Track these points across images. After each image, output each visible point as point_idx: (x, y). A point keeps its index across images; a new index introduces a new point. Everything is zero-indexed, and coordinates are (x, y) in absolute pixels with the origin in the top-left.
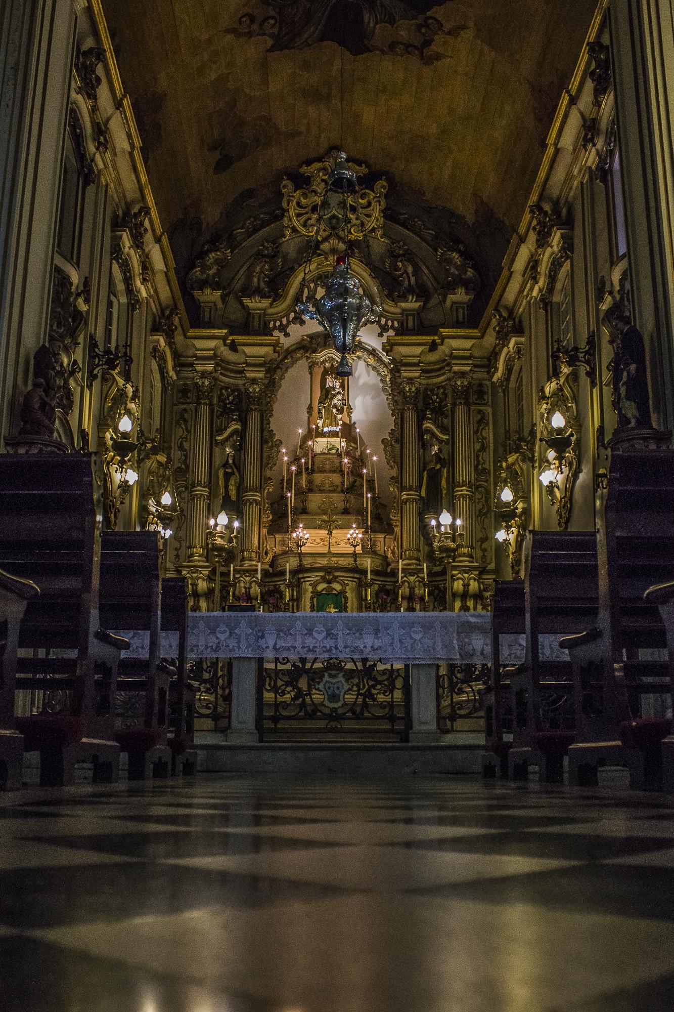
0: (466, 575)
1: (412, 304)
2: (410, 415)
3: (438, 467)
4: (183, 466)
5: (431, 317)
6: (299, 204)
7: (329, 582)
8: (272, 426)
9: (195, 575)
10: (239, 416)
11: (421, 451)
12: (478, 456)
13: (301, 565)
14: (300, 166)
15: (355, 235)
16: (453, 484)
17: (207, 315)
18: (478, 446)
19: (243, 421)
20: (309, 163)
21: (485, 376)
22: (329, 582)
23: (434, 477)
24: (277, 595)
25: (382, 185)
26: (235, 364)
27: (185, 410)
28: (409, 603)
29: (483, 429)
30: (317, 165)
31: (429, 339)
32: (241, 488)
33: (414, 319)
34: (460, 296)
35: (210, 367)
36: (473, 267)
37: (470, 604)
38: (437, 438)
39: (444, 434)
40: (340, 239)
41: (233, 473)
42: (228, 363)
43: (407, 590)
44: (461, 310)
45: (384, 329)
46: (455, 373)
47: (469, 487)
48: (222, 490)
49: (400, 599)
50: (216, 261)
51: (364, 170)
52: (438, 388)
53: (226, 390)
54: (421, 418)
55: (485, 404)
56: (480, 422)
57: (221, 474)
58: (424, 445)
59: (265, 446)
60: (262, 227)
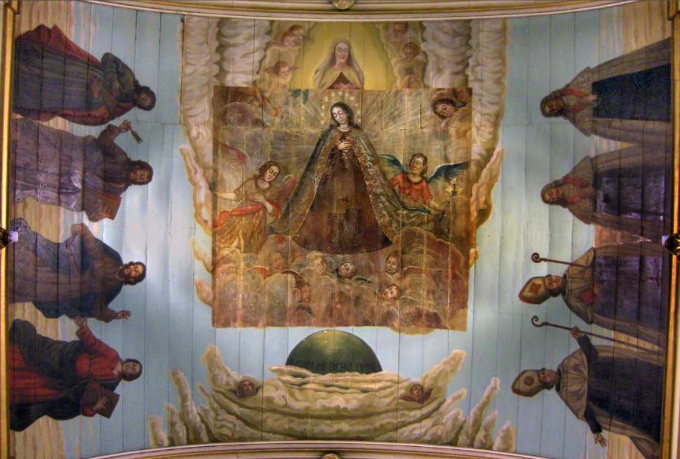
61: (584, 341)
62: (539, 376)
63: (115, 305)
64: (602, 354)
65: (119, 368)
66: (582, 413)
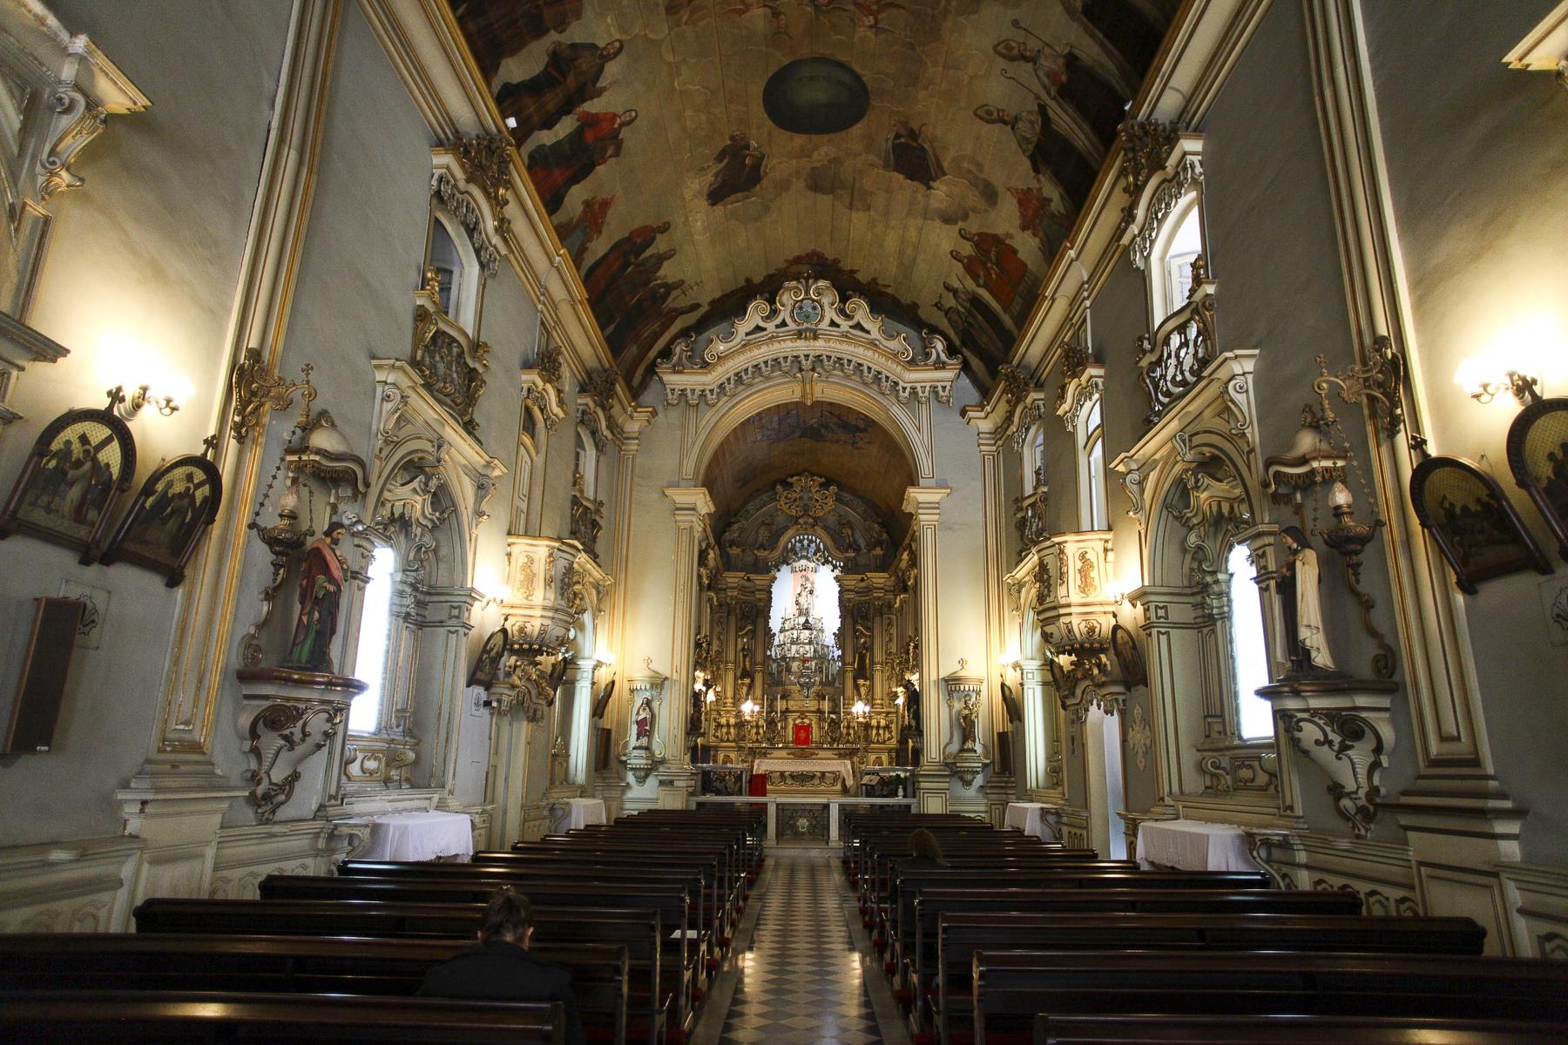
2: (849, 621)
5: (862, 560)
8: (770, 625)
13: (787, 708)
15: (820, 514)
16: (872, 663)
19: (754, 623)
20: (792, 476)
23: (862, 658)
25: (833, 488)
30: (795, 478)
32: (753, 664)
34: (878, 551)
35: (735, 594)
36: (887, 533)
37: (881, 732)
38: (864, 634)
40: (809, 516)
45: (835, 567)
51: (823, 480)
54: (855, 623)
56: (889, 624)
57: (741, 655)
58: (858, 638)
60: (764, 505)
61: (1043, 109)
62: (998, 112)
63: (600, 84)
64: (1054, 126)
65: (618, 121)
66: (1028, 154)
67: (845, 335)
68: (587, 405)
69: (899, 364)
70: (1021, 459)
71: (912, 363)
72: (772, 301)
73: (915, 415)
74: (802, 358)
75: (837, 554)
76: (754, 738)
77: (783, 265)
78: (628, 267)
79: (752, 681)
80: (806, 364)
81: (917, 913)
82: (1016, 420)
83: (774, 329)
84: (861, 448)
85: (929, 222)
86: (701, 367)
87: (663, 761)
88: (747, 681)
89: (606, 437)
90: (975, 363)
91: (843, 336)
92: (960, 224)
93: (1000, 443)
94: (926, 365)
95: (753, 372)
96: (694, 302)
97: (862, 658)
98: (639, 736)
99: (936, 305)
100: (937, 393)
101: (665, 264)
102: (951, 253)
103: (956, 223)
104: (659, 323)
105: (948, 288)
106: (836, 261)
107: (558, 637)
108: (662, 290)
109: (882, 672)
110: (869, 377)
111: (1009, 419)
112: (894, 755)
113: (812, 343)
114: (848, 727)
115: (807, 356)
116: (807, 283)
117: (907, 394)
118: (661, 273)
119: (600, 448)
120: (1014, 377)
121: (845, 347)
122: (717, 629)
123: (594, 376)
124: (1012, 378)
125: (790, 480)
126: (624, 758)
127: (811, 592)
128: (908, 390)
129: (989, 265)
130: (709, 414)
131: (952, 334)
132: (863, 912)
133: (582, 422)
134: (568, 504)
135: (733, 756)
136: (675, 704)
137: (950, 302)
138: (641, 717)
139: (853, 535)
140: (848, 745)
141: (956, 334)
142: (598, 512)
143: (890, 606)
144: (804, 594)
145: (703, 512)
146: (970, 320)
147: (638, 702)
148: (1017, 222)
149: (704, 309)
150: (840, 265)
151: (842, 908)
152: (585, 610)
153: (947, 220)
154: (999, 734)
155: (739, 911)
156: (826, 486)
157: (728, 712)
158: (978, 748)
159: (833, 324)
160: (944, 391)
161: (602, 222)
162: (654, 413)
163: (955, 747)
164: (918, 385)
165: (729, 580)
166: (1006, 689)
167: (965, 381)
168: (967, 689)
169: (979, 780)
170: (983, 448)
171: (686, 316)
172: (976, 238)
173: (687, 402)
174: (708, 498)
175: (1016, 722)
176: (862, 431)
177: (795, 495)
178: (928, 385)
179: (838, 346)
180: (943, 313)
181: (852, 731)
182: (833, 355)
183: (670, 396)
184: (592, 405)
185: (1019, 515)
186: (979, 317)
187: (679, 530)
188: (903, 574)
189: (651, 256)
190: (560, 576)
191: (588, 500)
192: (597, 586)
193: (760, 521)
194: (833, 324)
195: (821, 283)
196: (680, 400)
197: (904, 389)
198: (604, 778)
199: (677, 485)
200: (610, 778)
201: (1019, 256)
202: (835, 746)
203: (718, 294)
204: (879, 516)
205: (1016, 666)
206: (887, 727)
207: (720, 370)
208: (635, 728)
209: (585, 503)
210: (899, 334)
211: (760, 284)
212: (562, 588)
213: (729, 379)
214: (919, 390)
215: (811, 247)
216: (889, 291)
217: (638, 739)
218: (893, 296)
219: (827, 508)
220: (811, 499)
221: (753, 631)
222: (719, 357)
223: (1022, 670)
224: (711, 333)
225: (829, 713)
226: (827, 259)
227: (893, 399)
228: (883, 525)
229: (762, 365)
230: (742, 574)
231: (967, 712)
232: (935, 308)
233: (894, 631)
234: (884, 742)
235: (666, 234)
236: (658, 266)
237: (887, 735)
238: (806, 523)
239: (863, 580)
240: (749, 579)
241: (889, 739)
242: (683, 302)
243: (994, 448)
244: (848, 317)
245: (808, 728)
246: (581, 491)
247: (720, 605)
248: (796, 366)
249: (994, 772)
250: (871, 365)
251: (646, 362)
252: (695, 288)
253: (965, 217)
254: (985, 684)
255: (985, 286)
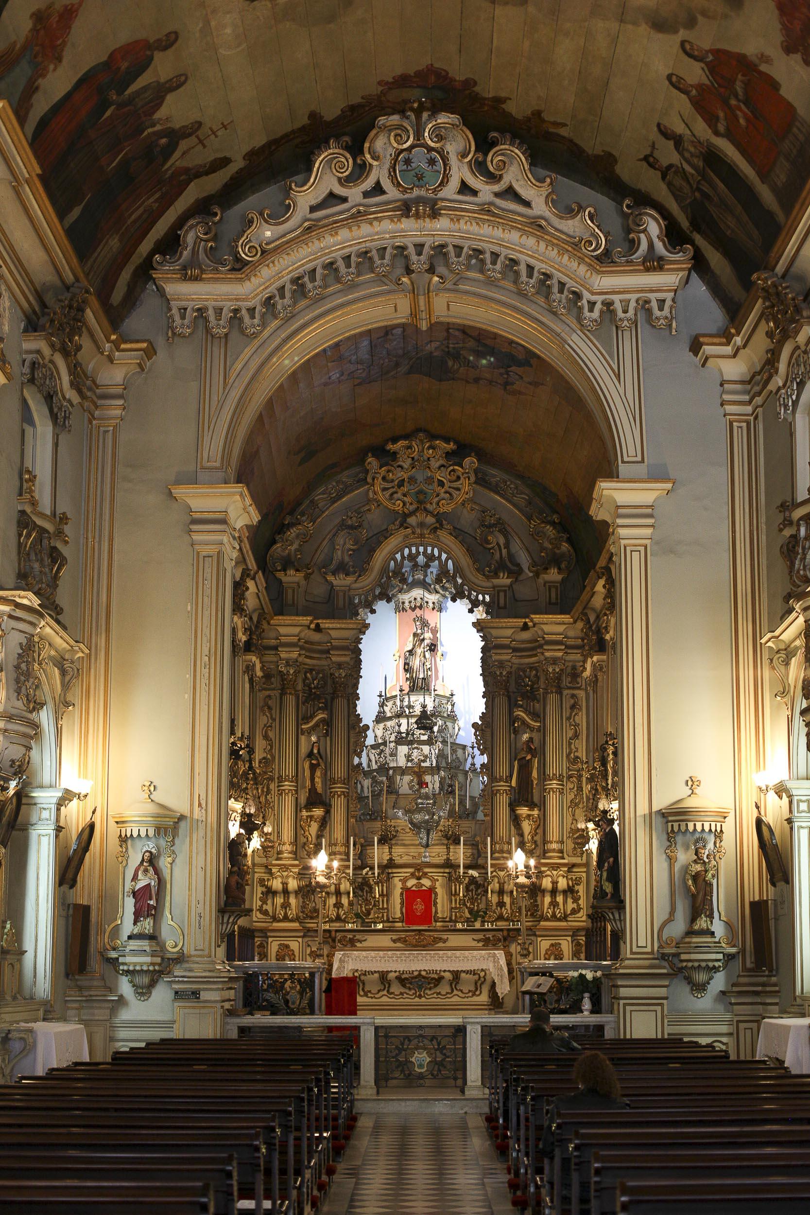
0: (555, 873)
1: (504, 580)
2: (501, 702)
3: (529, 757)
4: (269, 756)
5: (524, 591)
6: (384, 478)
7: (419, 878)
8: (359, 710)
9: (285, 874)
10: (326, 704)
11: (513, 736)
12: (570, 744)
13: (391, 860)
14: (386, 442)
15: (447, 508)
16: (544, 776)
17: (290, 596)
18: (570, 734)
19: (328, 707)
20: (395, 440)
21: (578, 657)
22: (419, 878)
23: (525, 768)
24: (366, 888)
25: (470, 462)
26: (319, 643)
27: (269, 697)
28: (499, 897)
29: (576, 714)
30: (401, 443)
31: (520, 622)
32: (329, 781)
33: (505, 596)
34: (554, 575)
35: (294, 655)
36: (569, 541)
37: (560, 899)
38: (528, 726)
39: (536, 721)
41: (318, 765)
42: (312, 643)
43: (497, 886)
44: (553, 590)
45: (475, 604)
46: (546, 659)
47: (559, 780)
48: (308, 783)
49: (490, 895)
50: (297, 536)
51: (452, 446)
52: (531, 668)
53: (311, 673)
54: (512, 705)
55: (579, 688)
56: (573, 707)
57: (307, 765)
58: (516, 732)
59: (351, 732)
67: (486, 210)
68: (38, 352)
69: (581, 260)
70: (792, 434)
71: (605, 259)
72: (356, 149)
73: (612, 351)
74: (411, 250)
75: (480, 580)
76: (333, 913)
77: (374, 90)
78: (109, 107)
79: (328, 812)
80: (418, 262)
81: (593, 1187)
82: (782, 366)
83: (359, 198)
84: (520, 393)
85: (630, 27)
86: (233, 269)
87: (180, 959)
88: (318, 812)
89: (69, 401)
90: (715, 258)
91: (483, 211)
92: (682, 34)
93: (758, 400)
94: (629, 262)
95: (324, 277)
96: (220, 155)
97: (525, 768)
98: (138, 916)
99: (646, 159)
100: (649, 312)
101: (170, 98)
102: (669, 77)
103: (676, 32)
104: (157, 196)
105: (665, 133)
106: (469, 83)
107: (13, 761)
108: (164, 141)
109: (561, 793)
110: (530, 285)
111: (771, 362)
112: (582, 940)
113: (428, 223)
114: (501, 892)
115: (419, 247)
116: (418, 117)
117: (596, 314)
118: (161, 113)
119: (60, 421)
120: (778, 294)
121: (486, 230)
122: (263, 720)
123: (49, 299)
124: (774, 296)
125: (390, 447)
126: (113, 955)
127: (433, 648)
128: (598, 306)
129: (733, 102)
130: (248, 352)
131: (673, 207)
132: (513, 1186)
133: (32, 381)
134: (13, 530)
135: (294, 945)
136: (199, 861)
137: (668, 155)
138: (141, 884)
139: (507, 546)
140: (501, 924)
141: (682, 208)
142: (60, 533)
143: (575, 675)
144: (419, 651)
145: (239, 525)
146: (706, 188)
147: (135, 858)
148: (778, 37)
149: (238, 164)
150: (477, 89)
151: (483, 1184)
152: (42, 705)
153: (660, 25)
154: (753, 904)
155: (322, 1187)
156: (456, 456)
157: (285, 868)
158: (718, 928)
159: (465, 188)
160: (661, 309)
161: (64, 43)
162: (150, 352)
163: (678, 927)
164: (616, 298)
165: (282, 630)
166: (765, 829)
167: (699, 289)
168: (699, 828)
169: (719, 982)
170: (729, 408)
171: (204, 178)
172: (710, 58)
173: (208, 330)
174: (248, 501)
175: (781, 884)
176: (520, 364)
177: (401, 474)
178: (633, 297)
179: (474, 228)
180: (659, 174)
181: (507, 899)
182: (466, 244)
183: (178, 321)
184: (47, 351)
185: (788, 532)
186: (721, 186)
187: (199, 559)
188: (598, 617)
189: (145, 89)
190: (13, 660)
191: (42, 515)
192: (60, 662)
193: (337, 520)
194: (465, 188)
195: (444, 118)
196: (195, 327)
197: (592, 305)
198: (80, 988)
199: (192, 480)
200: (89, 988)
201: (783, 92)
202: (478, 925)
203: (260, 141)
204: (555, 512)
205: (781, 790)
206: (570, 891)
207: (265, 272)
208: (129, 905)
209: (39, 522)
210: (581, 208)
211: (338, 119)
212: (17, 681)
213: (282, 289)
214: (618, 306)
215: (423, 63)
216: (563, 132)
217: (135, 923)
218: (571, 141)
219: (459, 497)
220: (429, 480)
221: (328, 723)
222: (263, 252)
223: (790, 796)
224: (249, 204)
225: (467, 867)
226: (452, 80)
227: (572, 321)
228: (562, 527)
229: (341, 264)
230: (305, 620)
231: (699, 868)
232: (644, 164)
233: (581, 718)
234: (565, 918)
235: (170, 52)
236: (158, 100)
237: (570, 905)
238: (422, 525)
239: (525, 627)
240: (318, 629)
241: (574, 911)
242: (199, 157)
243: (749, 409)
244: (492, 178)
245: (428, 895)
246: (34, 503)
247: (267, 676)
248: (400, 263)
249: (745, 969)
250: (532, 262)
251: (136, 260)
252: (219, 133)
253: (691, 23)
254: (730, 819)
255: (729, 135)
